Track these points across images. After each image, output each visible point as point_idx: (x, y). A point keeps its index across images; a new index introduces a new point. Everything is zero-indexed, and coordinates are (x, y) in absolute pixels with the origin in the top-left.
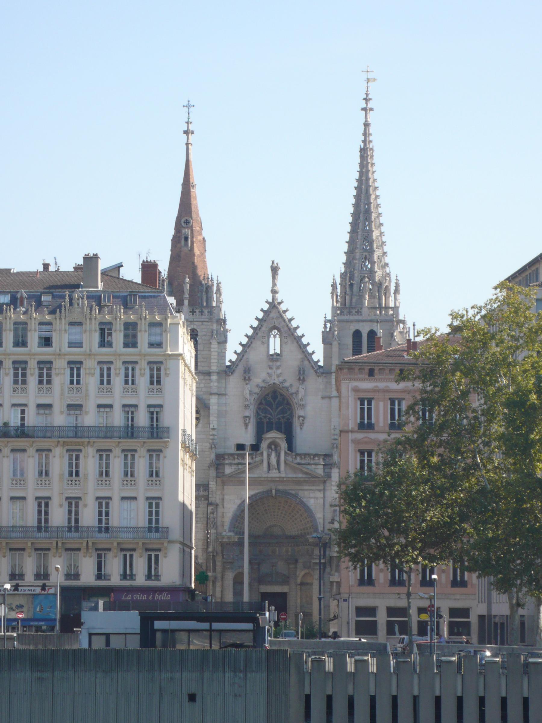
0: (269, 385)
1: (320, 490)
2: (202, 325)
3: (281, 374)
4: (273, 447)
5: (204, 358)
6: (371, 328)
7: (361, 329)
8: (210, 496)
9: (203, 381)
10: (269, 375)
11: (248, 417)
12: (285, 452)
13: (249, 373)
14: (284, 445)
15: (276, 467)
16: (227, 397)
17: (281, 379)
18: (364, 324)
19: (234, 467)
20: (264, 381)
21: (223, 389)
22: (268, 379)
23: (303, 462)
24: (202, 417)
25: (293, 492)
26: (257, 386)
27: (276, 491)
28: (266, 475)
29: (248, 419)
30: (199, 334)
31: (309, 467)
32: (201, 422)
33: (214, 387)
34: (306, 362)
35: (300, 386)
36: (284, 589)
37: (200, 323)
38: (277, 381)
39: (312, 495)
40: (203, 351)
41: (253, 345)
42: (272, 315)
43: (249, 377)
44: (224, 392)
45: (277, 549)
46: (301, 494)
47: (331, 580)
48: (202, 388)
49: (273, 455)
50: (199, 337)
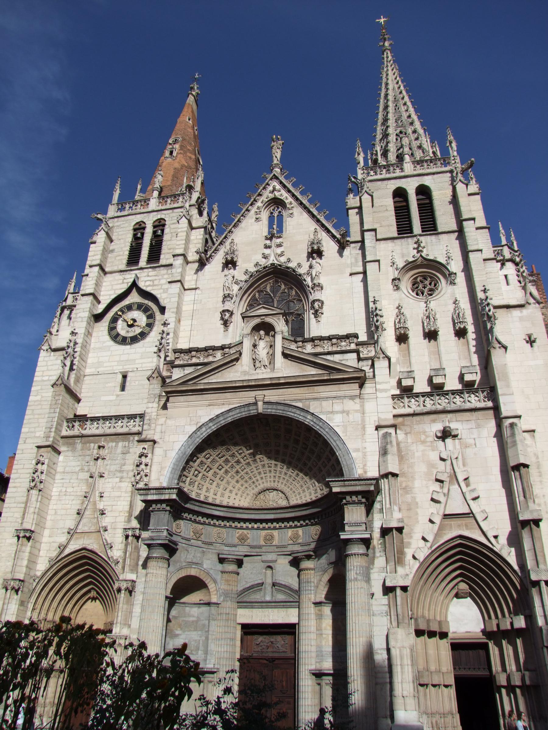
0: (264, 268)
1: (352, 398)
2: (173, 212)
4: (262, 332)
5: (170, 249)
6: (421, 183)
7: (404, 186)
8: (145, 427)
9: (166, 276)
10: (265, 257)
11: (228, 311)
12: (283, 338)
13: (233, 252)
14: (281, 326)
15: (267, 363)
16: (197, 291)
17: (283, 259)
18: (409, 179)
19: (189, 370)
20: (257, 265)
21: (193, 283)
22: (263, 262)
23: (319, 350)
24: (157, 323)
25: (300, 405)
27: (265, 403)
28: (247, 378)
29: (228, 315)
30: (166, 223)
31: (329, 357)
32: (155, 329)
33: (177, 275)
34: (323, 236)
35: (314, 261)
36: (288, 616)
37: (171, 211)
38: (276, 262)
39: (338, 407)
40: (171, 240)
41: (243, 225)
42: (271, 188)
43: (232, 258)
44: (194, 287)
45: (275, 533)
46: (314, 407)
47: (389, 584)
48: (162, 285)
50: (167, 226)
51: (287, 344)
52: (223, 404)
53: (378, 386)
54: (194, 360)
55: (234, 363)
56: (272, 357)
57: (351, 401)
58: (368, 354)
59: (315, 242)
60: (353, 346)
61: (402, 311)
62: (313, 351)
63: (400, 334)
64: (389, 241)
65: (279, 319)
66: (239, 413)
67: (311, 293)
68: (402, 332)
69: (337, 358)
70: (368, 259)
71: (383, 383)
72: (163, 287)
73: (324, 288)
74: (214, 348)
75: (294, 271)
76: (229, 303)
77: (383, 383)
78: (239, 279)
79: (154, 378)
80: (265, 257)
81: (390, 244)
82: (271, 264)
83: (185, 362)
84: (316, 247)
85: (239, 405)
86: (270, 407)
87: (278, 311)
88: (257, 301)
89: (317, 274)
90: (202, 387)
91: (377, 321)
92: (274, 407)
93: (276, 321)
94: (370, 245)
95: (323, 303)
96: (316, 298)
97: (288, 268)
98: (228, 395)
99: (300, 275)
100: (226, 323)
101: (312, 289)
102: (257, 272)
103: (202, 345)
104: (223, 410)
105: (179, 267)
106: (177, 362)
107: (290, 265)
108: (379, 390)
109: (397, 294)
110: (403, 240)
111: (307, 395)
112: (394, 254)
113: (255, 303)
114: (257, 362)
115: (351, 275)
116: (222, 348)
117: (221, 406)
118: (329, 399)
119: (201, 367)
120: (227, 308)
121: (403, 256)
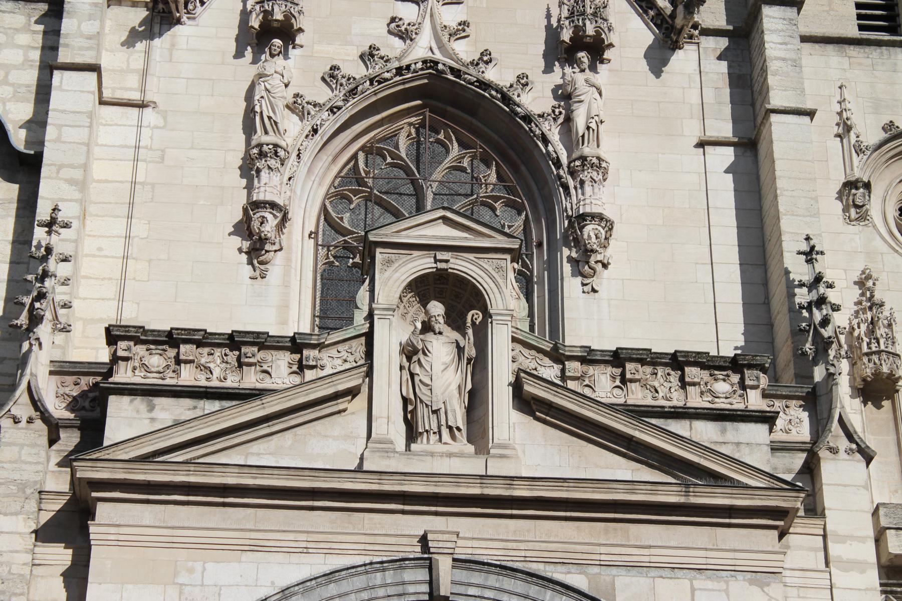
0: (399, 71)
3: (464, 24)
4: (437, 308)
11: (273, 205)
14: (504, 296)
17: (465, 51)
19: (169, 410)
20: (369, 56)
21: (133, 81)
22: (393, 47)
23: (638, 396)
26: (332, 76)
31: (679, 427)
43: (288, 16)
44: (135, 96)
49: (441, 350)
51: (529, 361)
52: (306, 551)
53: (834, 549)
54: (188, 377)
55: (341, 407)
56: (476, 400)
57: (755, 589)
58: (788, 432)
59: (589, 11)
60: (755, 401)
61: (878, 296)
62: (619, 398)
63: (877, 374)
64: (830, 48)
65: (498, 269)
66: (365, 589)
67: (566, 188)
68: (885, 369)
69: (705, 432)
70: (776, 99)
71: (852, 538)
72: (11, 78)
73: (610, 176)
74: (263, 341)
75: (506, 99)
76: (275, 178)
77: (852, 538)
78: (308, 98)
79: (16, 421)
80: (403, 32)
81: (832, 57)
82: (425, 62)
83: (153, 380)
84: (590, 30)
85: (367, 560)
86: (477, 578)
87: (500, 241)
88: (365, 185)
89: (593, 125)
90: (231, 480)
91: (825, 322)
92: (493, 580)
93: (492, 278)
94: (782, 54)
95: (609, 226)
96: (588, 210)
97: (485, 85)
98: (321, 521)
99: (528, 118)
100: (257, 248)
101: (573, 173)
102: (371, 81)
103: (160, 321)
104: (305, 573)
105: (91, 17)
106: (123, 375)
107: (491, 74)
108: (840, 560)
109: (855, 234)
110: (874, 53)
111: (603, 550)
112: (847, 96)
113: (355, 193)
114: (422, 411)
115: (701, 144)
116: (296, 345)
117: (295, 558)
118: (680, 573)
119: (216, 405)
120: (269, 197)
121: (877, 106)
